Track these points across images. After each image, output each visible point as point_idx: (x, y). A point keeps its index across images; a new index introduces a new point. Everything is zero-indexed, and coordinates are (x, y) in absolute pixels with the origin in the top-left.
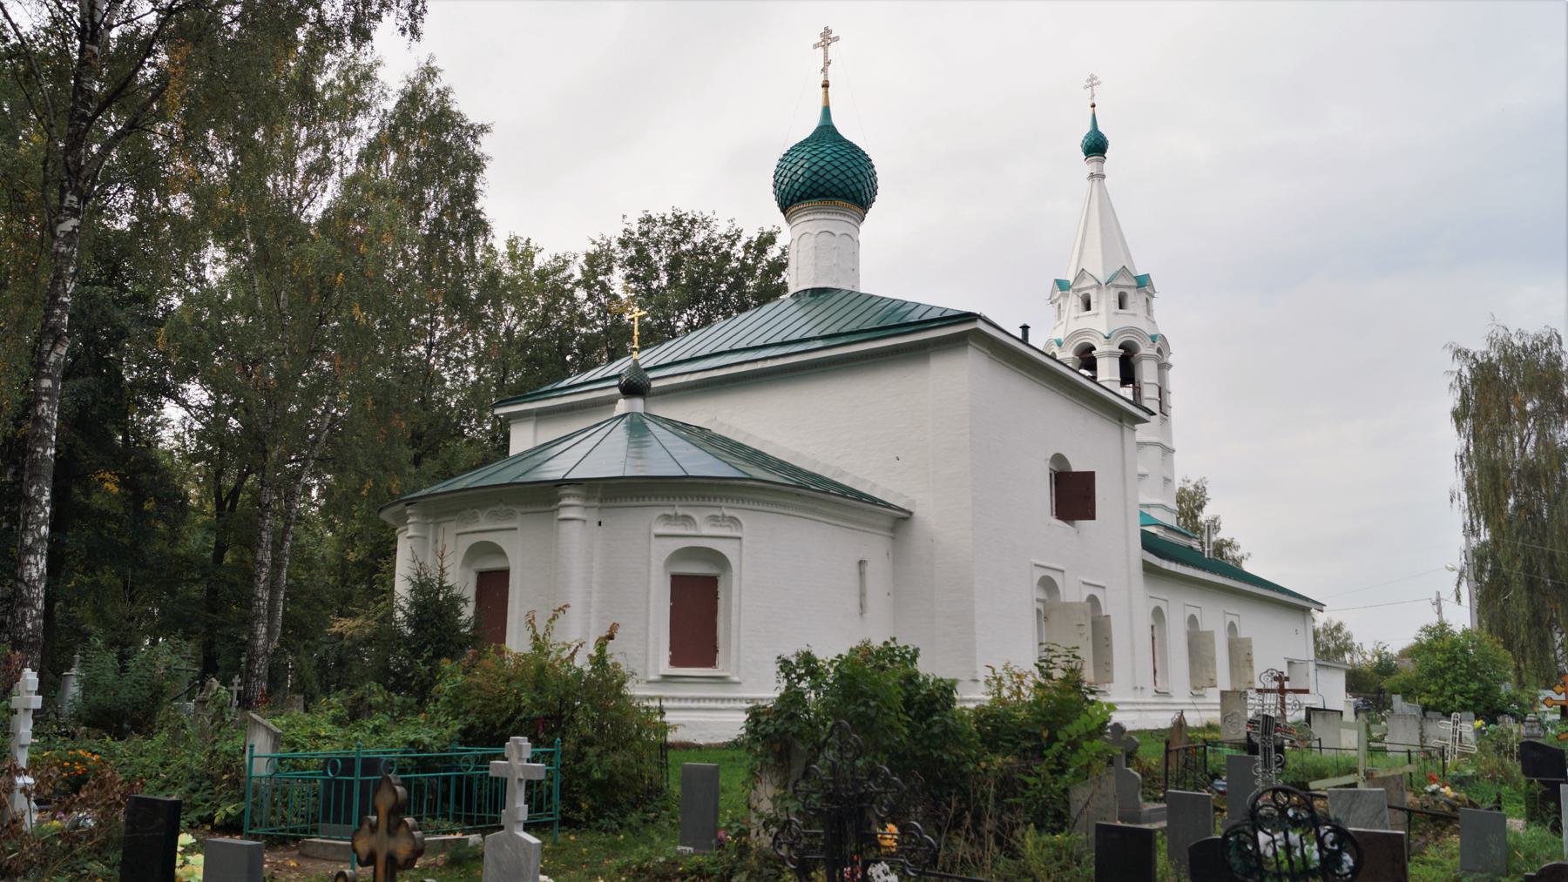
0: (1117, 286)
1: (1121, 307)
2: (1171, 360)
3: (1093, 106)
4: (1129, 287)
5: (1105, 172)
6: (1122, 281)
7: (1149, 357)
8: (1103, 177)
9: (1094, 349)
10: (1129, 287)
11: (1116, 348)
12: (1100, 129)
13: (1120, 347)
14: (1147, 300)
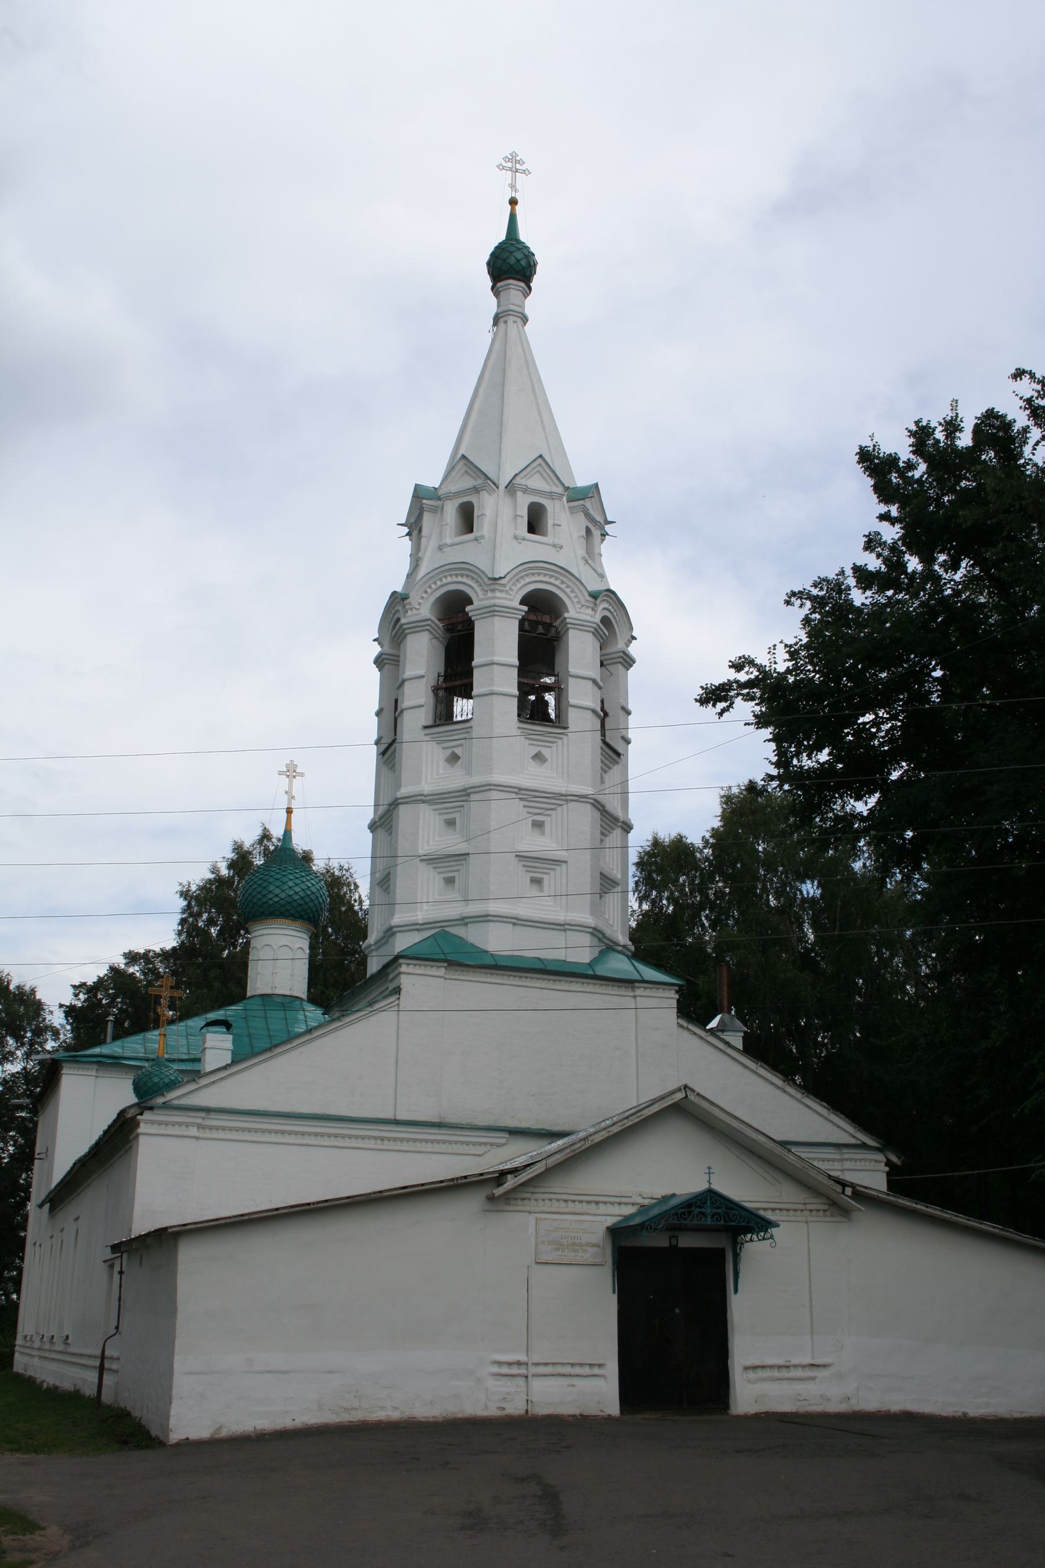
0: (526, 490)
1: (532, 528)
2: (633, 649)
3: (513, 202)
4: (551, 495)
5: (528, 312)
6: (535, 482)
7: (581, 626)
8: (525, 320)
9: (471, 602)
10: (551, 495)
11: (516, 603)
12: (523, 236)
13: (523, 602)
14: (588, 531)
